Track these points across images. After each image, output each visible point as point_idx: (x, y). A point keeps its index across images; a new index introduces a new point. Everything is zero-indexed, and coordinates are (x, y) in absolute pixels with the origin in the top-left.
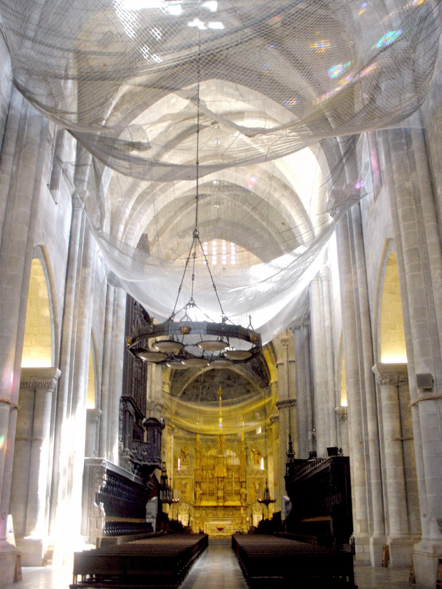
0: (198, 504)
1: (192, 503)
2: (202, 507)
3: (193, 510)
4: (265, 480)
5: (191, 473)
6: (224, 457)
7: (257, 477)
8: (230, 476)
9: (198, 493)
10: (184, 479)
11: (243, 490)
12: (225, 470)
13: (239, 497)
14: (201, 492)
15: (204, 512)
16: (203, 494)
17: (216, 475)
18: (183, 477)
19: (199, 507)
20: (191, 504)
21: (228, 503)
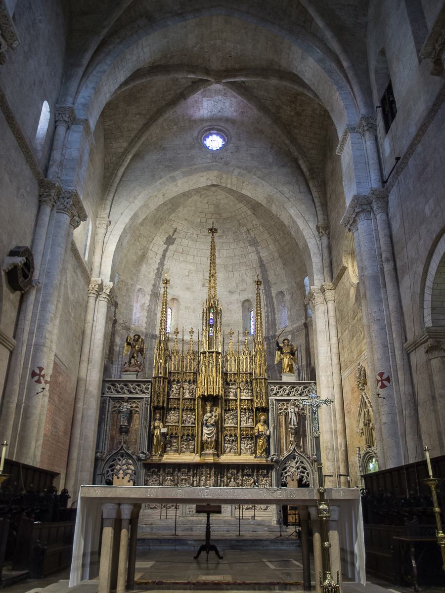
0: (156, 458)
3: (143, 472)
6: (218, 353)
9: (157, 432)
10: (129, 400)
14: (164, 430)
17: (199, 393)
20: (139, 459)
21: (225, 458)
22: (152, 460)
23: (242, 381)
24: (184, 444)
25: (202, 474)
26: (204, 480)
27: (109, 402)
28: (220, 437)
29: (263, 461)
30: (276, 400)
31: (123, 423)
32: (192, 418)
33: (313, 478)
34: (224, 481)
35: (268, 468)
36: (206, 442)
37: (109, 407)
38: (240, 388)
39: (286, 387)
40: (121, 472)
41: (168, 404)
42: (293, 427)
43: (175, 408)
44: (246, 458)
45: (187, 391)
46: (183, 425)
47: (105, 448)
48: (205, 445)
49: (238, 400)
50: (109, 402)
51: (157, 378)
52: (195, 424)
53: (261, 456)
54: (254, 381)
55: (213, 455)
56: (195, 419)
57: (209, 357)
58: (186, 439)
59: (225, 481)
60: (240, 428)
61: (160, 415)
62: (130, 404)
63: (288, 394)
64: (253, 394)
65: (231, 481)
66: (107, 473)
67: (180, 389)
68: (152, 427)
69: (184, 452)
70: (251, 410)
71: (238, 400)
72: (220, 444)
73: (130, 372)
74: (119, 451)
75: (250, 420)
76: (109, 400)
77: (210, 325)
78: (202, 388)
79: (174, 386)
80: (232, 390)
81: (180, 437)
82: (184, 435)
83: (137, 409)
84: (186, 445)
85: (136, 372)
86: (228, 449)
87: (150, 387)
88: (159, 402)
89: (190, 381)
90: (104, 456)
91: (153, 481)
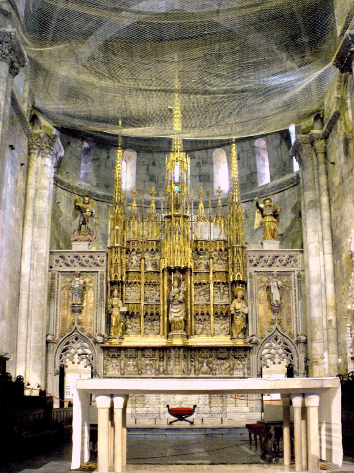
0: (115, 342)
1: (100, 339)
2: (126, 348)
3: (101, 357)
4: (293, 277)
5: (98, 259)
7: (274, 269)
8: (202, 269)
9: (116, 312)
11: (238, 305)
12: (189, 250)
13: (226, 324)
14: (124, 309)
15: (131, 362)
16: (128, 315)
17: (164, 265)
18: (78, 269)
19: (120, 349)
20: (96, 342)
21: (195, 341)
22: (111, 343)
23: (216, 251)
24: (147, 325)
25: (169, 358)
26: (172, 365)
27: (58, 277)
28: (189, 316)
29: (240, 343)
30: (255, 271)
31: (76, 301)
32: (156, 294)
33: (298, 361)
34: (195, 366)
35: (246, 349)
36: (173, 322)
37: (58, 283)
38: (213, 258)
39: (268, 257)
40: (76, 356)
41: (127, 279)
42: (275, 302)
43: (135, 283)
44: (223, 340)
45: (150, 263)
46: (146, 303)
47: (56, 330)
48: (173, 325)
49: (211, 273)
50: (58, 277)
51: (114, 249)
52: (159, 301)
53: (238, 338)
54: (230, 250)
55: (182, 337)
56: (159, 296)
57: (176, 221)
58: (149, 319)
59: (197, 366)
60: (214, 304)
61: (119, 291)
62: (83, 279)
63: (270, 265)
64: (228, 265)
65: (203, 366)
66: (61, 358)
67: (141, 260)
68: (109, 306)
69: (148, 334)
70: (226, 284)
71: (211, 273)
72: (189, 323)
73: (81, 241)
74: (73, 333)
75: (225, 297)
76: (58, 274)
77: (176, 183)
78: (168, 259)
79: (134, 257)
80: (203, 261)
81: (142, 317)
82: (147, 314)
83: (91, 285)
84: (150, 326)
85: (88, 241)
86: (200, 330)
87: (105, 259)
88: (116, 276)
89: (152, 250)
90: (56, 339)
91: (113, 366)
